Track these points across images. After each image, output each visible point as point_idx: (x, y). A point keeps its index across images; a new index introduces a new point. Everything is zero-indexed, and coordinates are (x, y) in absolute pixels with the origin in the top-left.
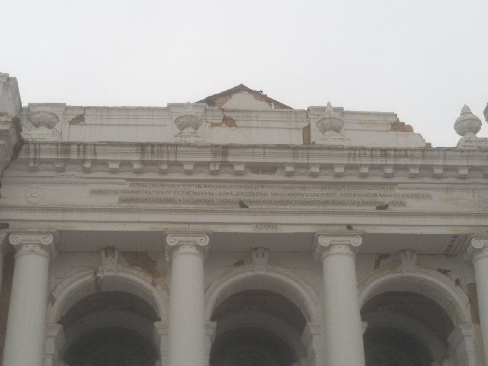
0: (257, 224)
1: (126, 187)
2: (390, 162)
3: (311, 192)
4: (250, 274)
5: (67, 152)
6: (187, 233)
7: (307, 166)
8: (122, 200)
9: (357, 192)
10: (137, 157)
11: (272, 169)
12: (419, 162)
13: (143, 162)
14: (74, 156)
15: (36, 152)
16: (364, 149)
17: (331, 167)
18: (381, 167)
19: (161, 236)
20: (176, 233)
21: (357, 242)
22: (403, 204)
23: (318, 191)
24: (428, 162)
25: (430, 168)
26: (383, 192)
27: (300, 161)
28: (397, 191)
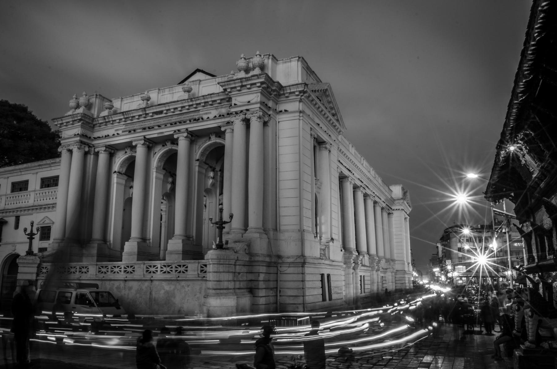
0: (158, 133)
1: (124, 127)
2: (194, 103)
3: (174, 118)
4: (167, 149)
5: (105, 119)
6: (138, 140)
7: (169, 110)
8: (123, 132)
9: (188, 115)
10: (122, 117)
11: (161, 112)
12: (203, 101)
13: (125, 118)
14: (107, 120)
15: (98, 121)
16: (184, 100)
17: (176, 108)
18: (192, 105)
19: (131, 142)
20: (135, 141)
21: (185, 134)
23: (176, 118)
24: (206, 100)
25: (207, 102)
26: (196, 114)
27: (167, 108)
28: (201, 113)
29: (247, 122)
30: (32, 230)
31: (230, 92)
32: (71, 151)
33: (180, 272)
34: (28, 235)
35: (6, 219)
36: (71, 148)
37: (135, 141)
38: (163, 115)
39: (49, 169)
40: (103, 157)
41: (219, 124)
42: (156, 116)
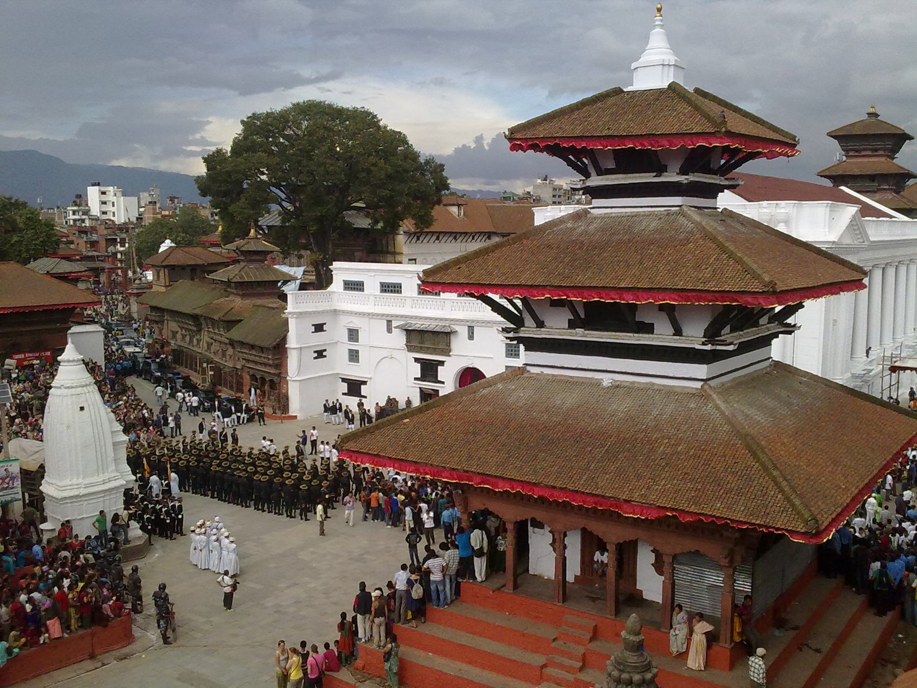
35: (456, 328)
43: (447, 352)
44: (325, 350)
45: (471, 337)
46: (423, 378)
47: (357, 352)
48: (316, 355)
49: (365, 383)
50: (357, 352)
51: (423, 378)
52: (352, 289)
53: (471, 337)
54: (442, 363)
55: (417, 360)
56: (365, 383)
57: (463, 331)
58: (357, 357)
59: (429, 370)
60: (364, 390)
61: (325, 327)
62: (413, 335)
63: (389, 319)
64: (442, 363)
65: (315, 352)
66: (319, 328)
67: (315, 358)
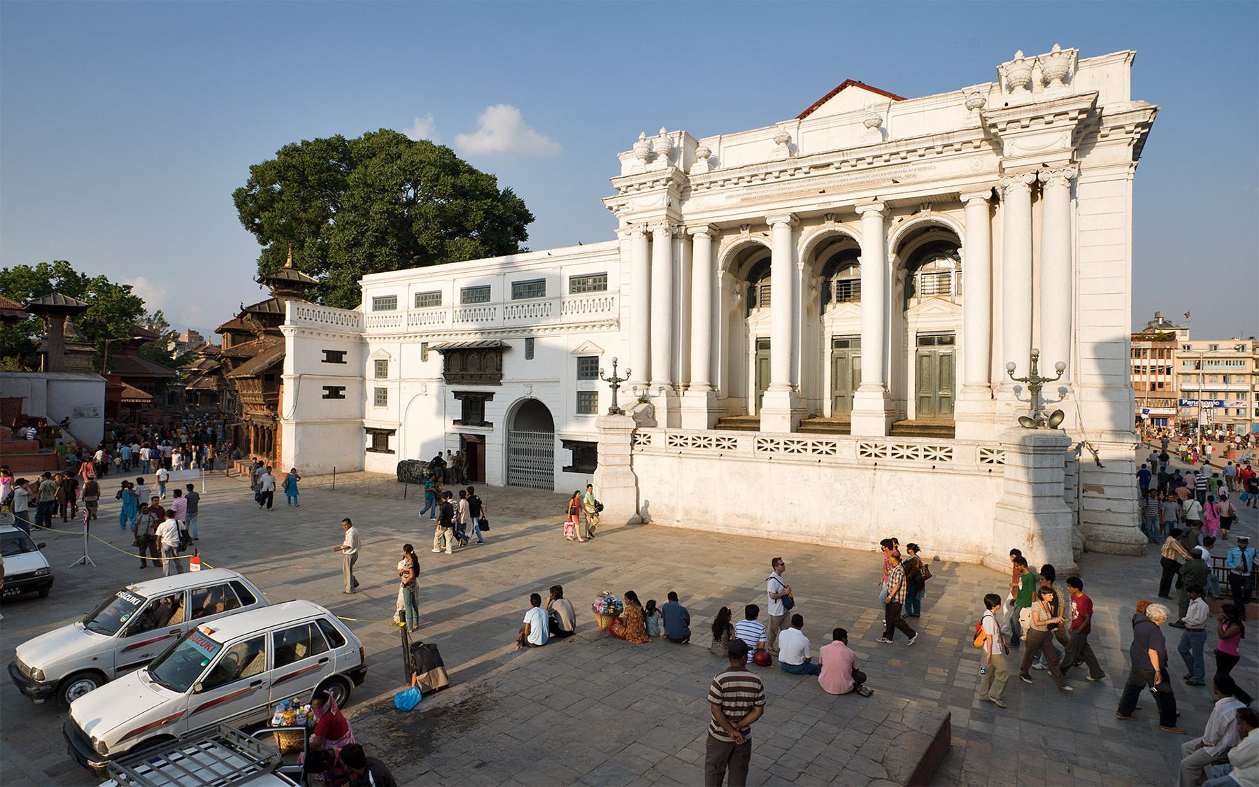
11: (828, 165)
20: (772, 216)
22: (914, 176)
28: (911, 167)
29: (1036, 189)
30: (615, 374)
31: (1004, 130)
32: (649, 237)
33: (935, 458)
34: (609, 380)
36: (649, 230)
37: (772, 216)
38: (831, 170)
39: (585, 261)
40: (701, 244)
41: (955, 190)
42: (814, 172)
43: (496, 377)
44: (344, 388)
45: (530, 354)
46: (464, 421)
47: (385, 390)
48: (327, 392)
49: (392, 432)
50: (385, 390)
51: (464, 421)
52: (383, 308)
53: (530, 354)
54: (490, 396)
55: (457, 395)
56: (392, 432)
57: (519, 346)
58: (385, 397)
59: (473, 408)
60: (393, 442)
61: (344, 358)
62: (456, 360)
63: (424, 340)
64: (490, 396)
65: (325, 388)
66: (334, 357)
67: (324, 397)
